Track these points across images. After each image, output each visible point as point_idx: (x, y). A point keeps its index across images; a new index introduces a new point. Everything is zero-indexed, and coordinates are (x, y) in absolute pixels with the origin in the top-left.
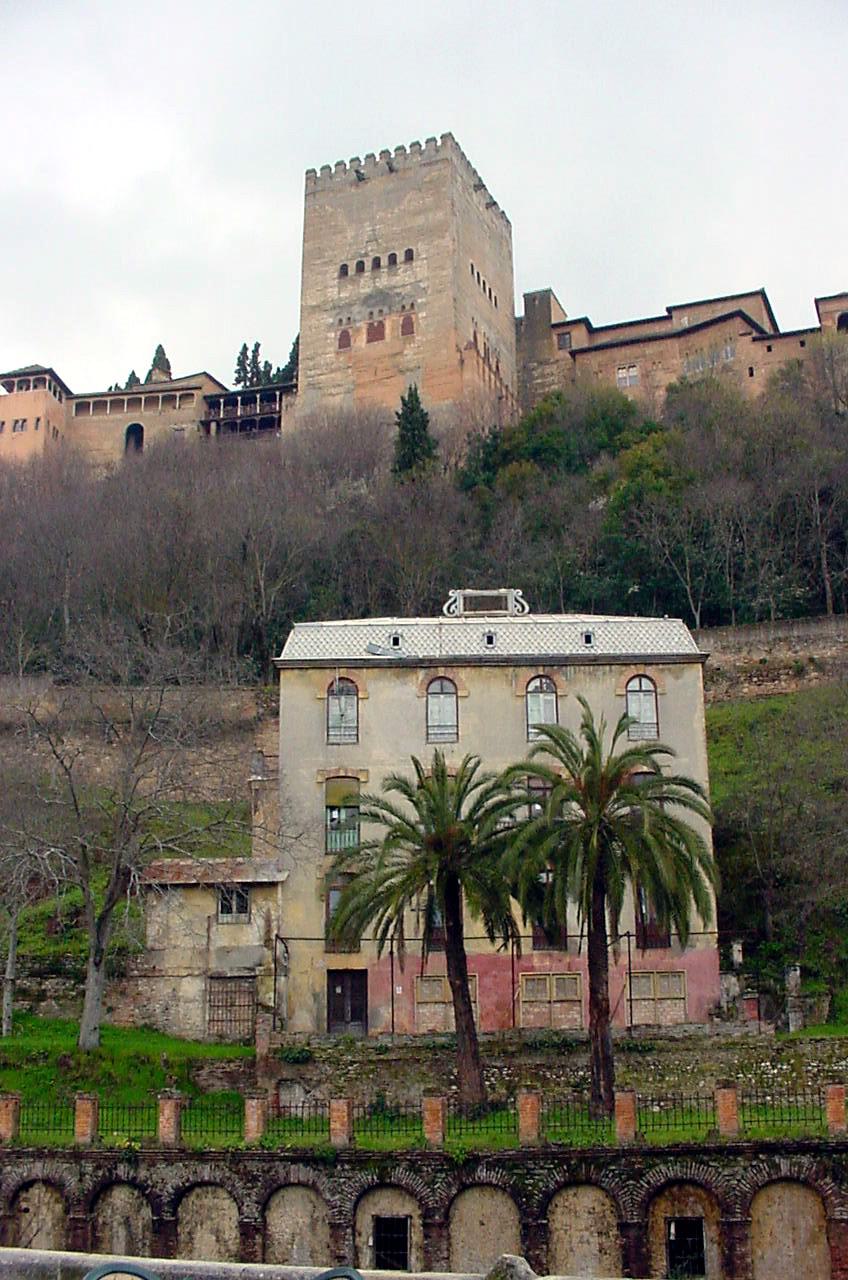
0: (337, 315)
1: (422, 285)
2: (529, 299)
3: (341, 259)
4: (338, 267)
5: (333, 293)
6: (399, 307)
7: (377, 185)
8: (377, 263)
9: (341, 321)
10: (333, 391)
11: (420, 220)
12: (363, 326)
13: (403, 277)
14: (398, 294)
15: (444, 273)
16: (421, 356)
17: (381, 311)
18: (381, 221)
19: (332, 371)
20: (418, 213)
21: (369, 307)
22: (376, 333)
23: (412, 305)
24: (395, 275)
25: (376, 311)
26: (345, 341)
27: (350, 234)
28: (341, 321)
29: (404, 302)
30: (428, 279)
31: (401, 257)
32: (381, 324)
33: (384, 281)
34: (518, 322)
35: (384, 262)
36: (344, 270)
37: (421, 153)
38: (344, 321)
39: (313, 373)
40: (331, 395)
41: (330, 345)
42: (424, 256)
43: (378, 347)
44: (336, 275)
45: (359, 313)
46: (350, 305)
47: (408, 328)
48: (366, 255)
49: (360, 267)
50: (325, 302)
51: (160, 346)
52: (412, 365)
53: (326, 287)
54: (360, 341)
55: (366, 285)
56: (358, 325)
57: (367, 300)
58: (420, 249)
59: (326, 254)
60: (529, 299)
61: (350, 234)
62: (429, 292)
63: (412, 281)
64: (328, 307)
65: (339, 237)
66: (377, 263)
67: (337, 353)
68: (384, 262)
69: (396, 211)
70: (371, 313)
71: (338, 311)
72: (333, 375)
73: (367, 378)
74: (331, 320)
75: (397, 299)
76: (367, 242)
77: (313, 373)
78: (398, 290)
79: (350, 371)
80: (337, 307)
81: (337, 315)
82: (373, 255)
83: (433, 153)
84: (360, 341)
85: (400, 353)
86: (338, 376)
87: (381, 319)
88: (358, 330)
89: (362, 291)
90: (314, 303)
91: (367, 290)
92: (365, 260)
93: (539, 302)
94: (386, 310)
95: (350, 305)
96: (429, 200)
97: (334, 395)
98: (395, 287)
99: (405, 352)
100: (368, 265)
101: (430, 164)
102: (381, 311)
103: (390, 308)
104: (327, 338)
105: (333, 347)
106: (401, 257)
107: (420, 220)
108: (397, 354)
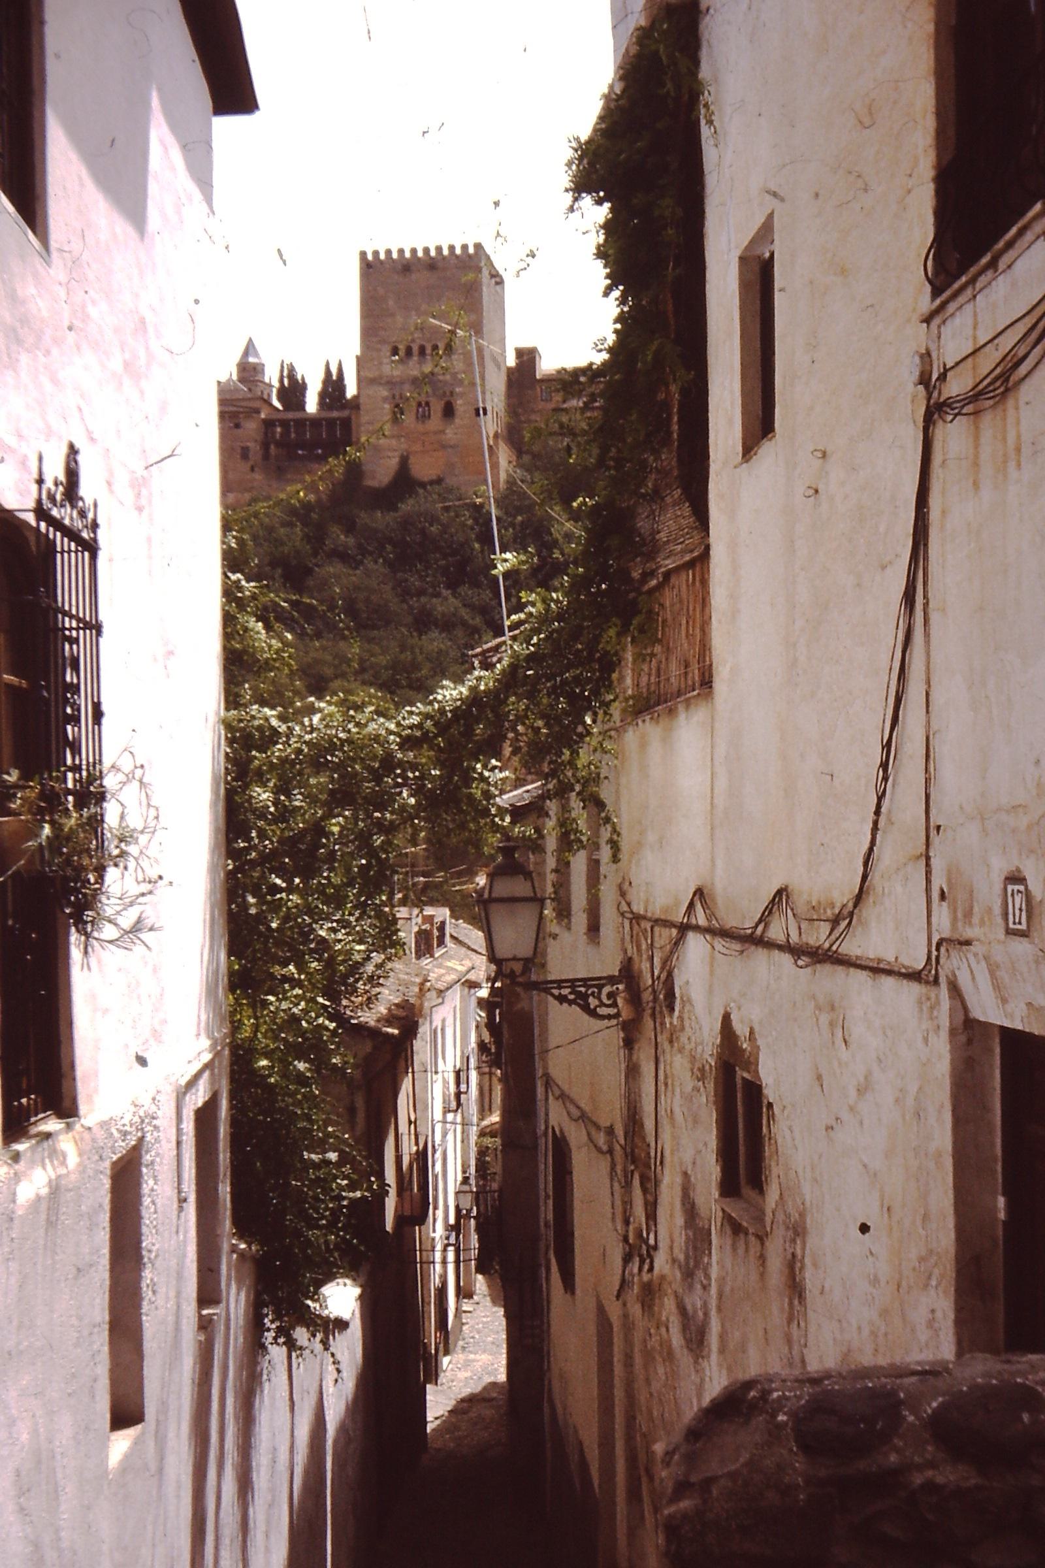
2: (520, 353)
5: (387, 370)
7: (421, 278)
8: (422, 350)
9: (394, 397)
10: (390, 454)
27: (399, 319)
34: (510, 371)
36: (395, 351)
37: (457, 257)
38: (397, 397)
46: (402, 383)
47: (449, 411)
48: (413, 341)
49: (409, 352)
50: (381, 377)
51: (250, 340)
55: (414, 368)
57: (415, 382)
60: (520, 353)
66: (422, 350)
74: (386, 393)
80: (390, 383)
82: (419, 342)
85: (443, 432)
93: (527, 357)
95: (402, 383)
100: (415, 349)
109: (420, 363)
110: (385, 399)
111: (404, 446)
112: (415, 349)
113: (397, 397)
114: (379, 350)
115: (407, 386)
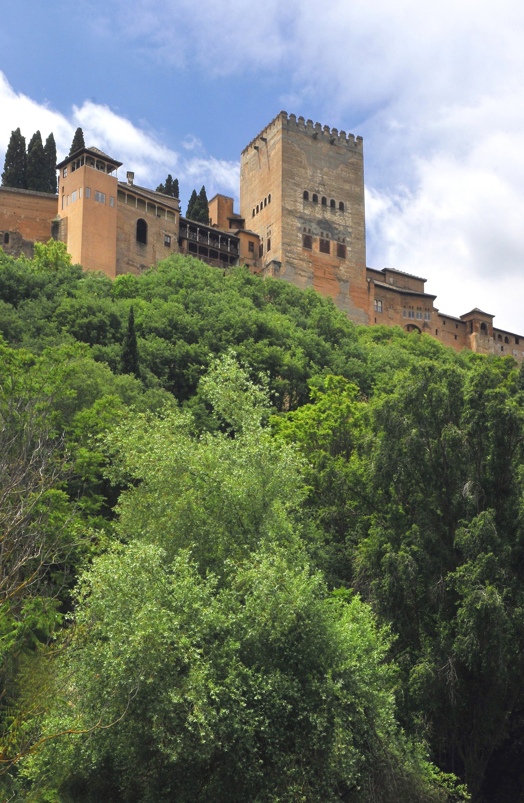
0: (303, 223)
1: (350, 230)
3: (305, 186)
4: (303, 191)
6: (336, 237)
9: (305, 229)
11: (347, 187)
12: (318, 238)
13: (336, 218)
14: (337, 229)
15: (360, 228)
16: (348, 275)
17: (327, 235)
18: (327, 174)
19: (301, 260)
20: (346, 181)
21: (321, 228)
22: (325, 248)
23: (344, 240)
24: (335, 215)
25: (325, 233)
26: (307, 243)
28: (305, 229)
29: (340, 235)
30: (351, 227)
31: (337, 206)
32: (328, 243)
33: (328, 215)
35: (329, 203)
36: (306, 196)
37: (347, 141)
38: (307, 230)
39: (289, 255)
40: (300, 274)
41: (300, 242)
42: (350, 211)
43: (324, 256)
44: (302, 195)
45: (315, 229)
47: (341, 252)
48: (318, 192)
52: (344, 278)
53: (296, 201)
54: (316, 246)
55: (318, 212)
56: (315, 237)
58: (347, 204)
59: (297, 178)
61: (309, 173)
62: (353, 236)
63: (343, 223)
64: (298, 215)
65: (303, 171)
67: (304, 250)
68: (329, 203)
69: (334, 172)
70: (322, 233)
71: (302, 221)
72: (301, 262)
73: (320, 274)
74: (300, 225)
75: (336, 232)
76: (319, 184)
77: (289, 255)
78: (337, 227)
79: (311, 265)
81: (303, 223)
83: (353, 145)
84: (316, 246)
85: (338, 267)
86: (304, 264)
87: (328, 239)
88: (315, 240)
89: (317, 215)
90: (290, 208)
91: (319, 216)
92: (318, 195)
94: (330, 235)
95: (310, 221)
96: (352, 176)
97: (302, 276)
98: (335, 223)
99: (341, 268)
100: (320, 200)
101: (352, 152)
102: (327, 235)
103: (332, 235)
104: (297, 236)
105: (301, 244)
106: (337, 206)
107: (347, 187)
108: (335, 267)
109: (324, 211)
110: (299, 229)
111: (312, 270)
112: (320, 200)
113: (307, 230)
114: (296, 191)
115: (314, 226)
